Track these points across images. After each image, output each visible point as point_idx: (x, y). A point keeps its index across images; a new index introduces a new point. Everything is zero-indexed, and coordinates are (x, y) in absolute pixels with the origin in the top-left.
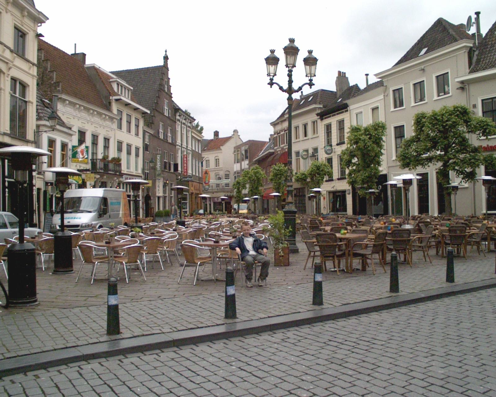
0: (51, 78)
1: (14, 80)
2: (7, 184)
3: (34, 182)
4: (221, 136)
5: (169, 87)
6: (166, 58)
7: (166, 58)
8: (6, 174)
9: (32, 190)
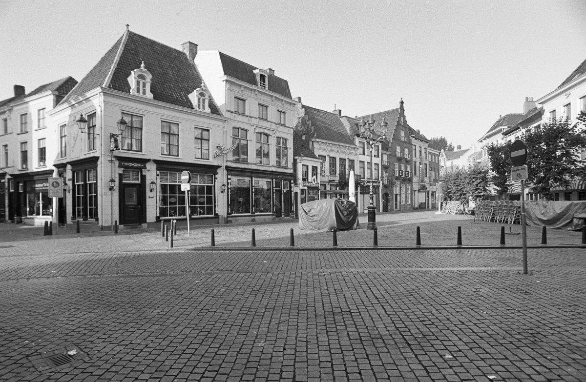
0: (311, 130)
1: (279, 138)
2: (274, 191)
3: (292, 189)
4: (463, 148)
5: (405, 122)
6: (402, 103)
7: (402, 103)
8: (274, 186)
9: (291, 194)
